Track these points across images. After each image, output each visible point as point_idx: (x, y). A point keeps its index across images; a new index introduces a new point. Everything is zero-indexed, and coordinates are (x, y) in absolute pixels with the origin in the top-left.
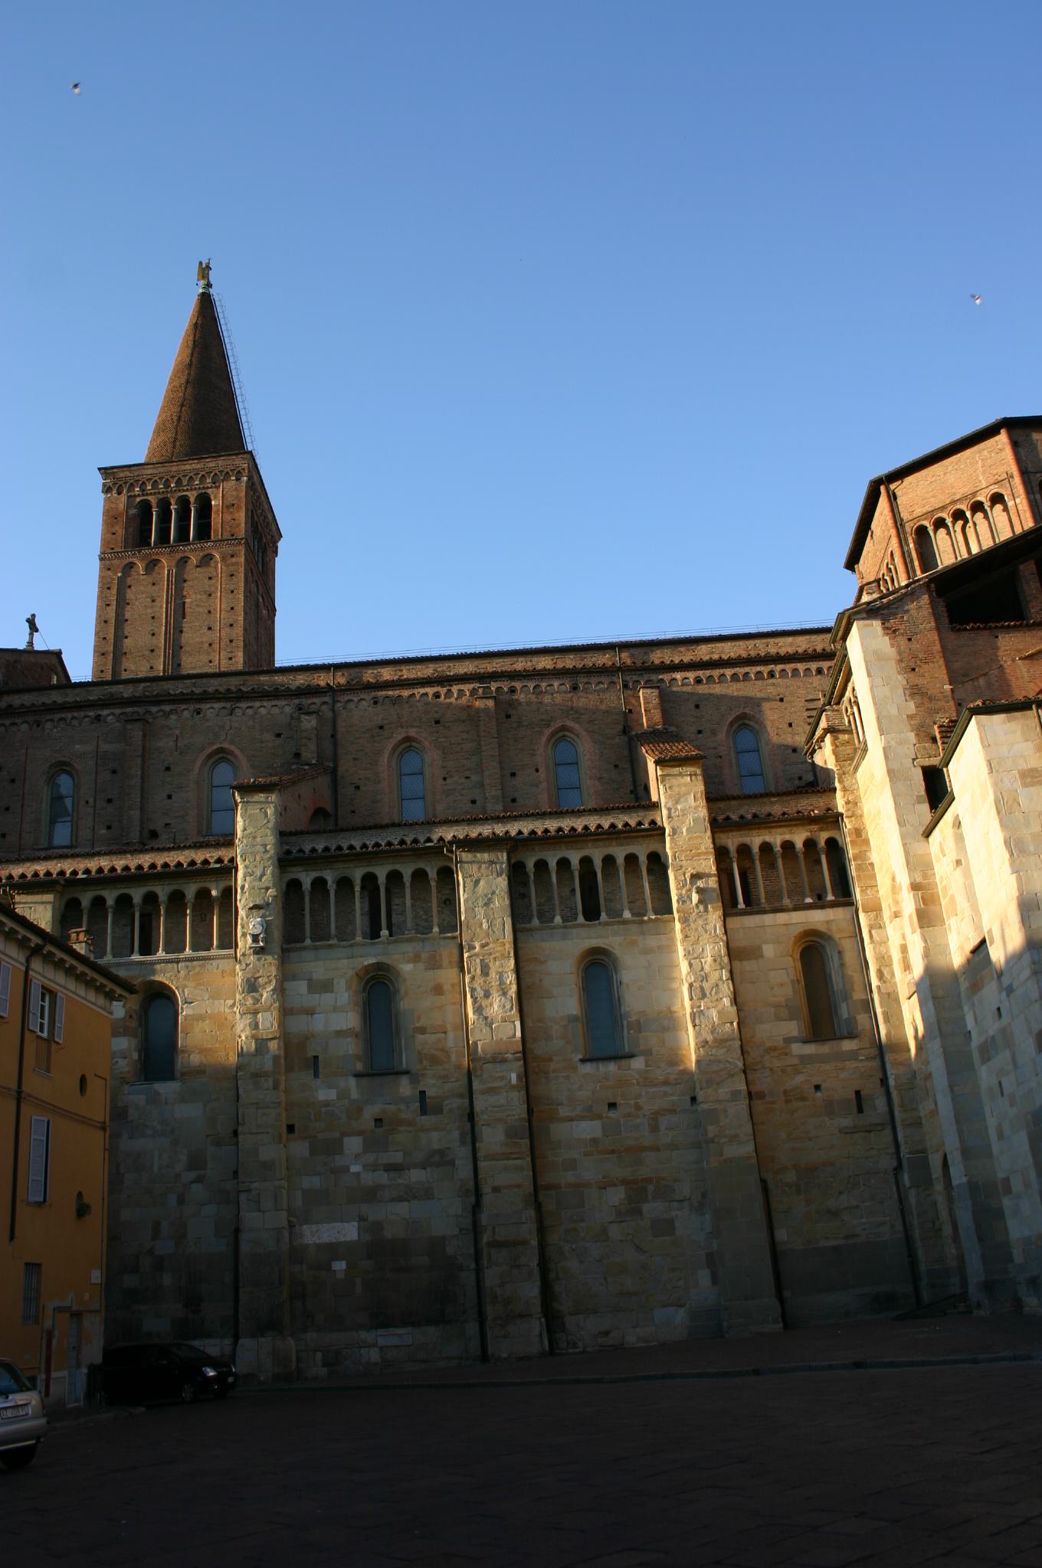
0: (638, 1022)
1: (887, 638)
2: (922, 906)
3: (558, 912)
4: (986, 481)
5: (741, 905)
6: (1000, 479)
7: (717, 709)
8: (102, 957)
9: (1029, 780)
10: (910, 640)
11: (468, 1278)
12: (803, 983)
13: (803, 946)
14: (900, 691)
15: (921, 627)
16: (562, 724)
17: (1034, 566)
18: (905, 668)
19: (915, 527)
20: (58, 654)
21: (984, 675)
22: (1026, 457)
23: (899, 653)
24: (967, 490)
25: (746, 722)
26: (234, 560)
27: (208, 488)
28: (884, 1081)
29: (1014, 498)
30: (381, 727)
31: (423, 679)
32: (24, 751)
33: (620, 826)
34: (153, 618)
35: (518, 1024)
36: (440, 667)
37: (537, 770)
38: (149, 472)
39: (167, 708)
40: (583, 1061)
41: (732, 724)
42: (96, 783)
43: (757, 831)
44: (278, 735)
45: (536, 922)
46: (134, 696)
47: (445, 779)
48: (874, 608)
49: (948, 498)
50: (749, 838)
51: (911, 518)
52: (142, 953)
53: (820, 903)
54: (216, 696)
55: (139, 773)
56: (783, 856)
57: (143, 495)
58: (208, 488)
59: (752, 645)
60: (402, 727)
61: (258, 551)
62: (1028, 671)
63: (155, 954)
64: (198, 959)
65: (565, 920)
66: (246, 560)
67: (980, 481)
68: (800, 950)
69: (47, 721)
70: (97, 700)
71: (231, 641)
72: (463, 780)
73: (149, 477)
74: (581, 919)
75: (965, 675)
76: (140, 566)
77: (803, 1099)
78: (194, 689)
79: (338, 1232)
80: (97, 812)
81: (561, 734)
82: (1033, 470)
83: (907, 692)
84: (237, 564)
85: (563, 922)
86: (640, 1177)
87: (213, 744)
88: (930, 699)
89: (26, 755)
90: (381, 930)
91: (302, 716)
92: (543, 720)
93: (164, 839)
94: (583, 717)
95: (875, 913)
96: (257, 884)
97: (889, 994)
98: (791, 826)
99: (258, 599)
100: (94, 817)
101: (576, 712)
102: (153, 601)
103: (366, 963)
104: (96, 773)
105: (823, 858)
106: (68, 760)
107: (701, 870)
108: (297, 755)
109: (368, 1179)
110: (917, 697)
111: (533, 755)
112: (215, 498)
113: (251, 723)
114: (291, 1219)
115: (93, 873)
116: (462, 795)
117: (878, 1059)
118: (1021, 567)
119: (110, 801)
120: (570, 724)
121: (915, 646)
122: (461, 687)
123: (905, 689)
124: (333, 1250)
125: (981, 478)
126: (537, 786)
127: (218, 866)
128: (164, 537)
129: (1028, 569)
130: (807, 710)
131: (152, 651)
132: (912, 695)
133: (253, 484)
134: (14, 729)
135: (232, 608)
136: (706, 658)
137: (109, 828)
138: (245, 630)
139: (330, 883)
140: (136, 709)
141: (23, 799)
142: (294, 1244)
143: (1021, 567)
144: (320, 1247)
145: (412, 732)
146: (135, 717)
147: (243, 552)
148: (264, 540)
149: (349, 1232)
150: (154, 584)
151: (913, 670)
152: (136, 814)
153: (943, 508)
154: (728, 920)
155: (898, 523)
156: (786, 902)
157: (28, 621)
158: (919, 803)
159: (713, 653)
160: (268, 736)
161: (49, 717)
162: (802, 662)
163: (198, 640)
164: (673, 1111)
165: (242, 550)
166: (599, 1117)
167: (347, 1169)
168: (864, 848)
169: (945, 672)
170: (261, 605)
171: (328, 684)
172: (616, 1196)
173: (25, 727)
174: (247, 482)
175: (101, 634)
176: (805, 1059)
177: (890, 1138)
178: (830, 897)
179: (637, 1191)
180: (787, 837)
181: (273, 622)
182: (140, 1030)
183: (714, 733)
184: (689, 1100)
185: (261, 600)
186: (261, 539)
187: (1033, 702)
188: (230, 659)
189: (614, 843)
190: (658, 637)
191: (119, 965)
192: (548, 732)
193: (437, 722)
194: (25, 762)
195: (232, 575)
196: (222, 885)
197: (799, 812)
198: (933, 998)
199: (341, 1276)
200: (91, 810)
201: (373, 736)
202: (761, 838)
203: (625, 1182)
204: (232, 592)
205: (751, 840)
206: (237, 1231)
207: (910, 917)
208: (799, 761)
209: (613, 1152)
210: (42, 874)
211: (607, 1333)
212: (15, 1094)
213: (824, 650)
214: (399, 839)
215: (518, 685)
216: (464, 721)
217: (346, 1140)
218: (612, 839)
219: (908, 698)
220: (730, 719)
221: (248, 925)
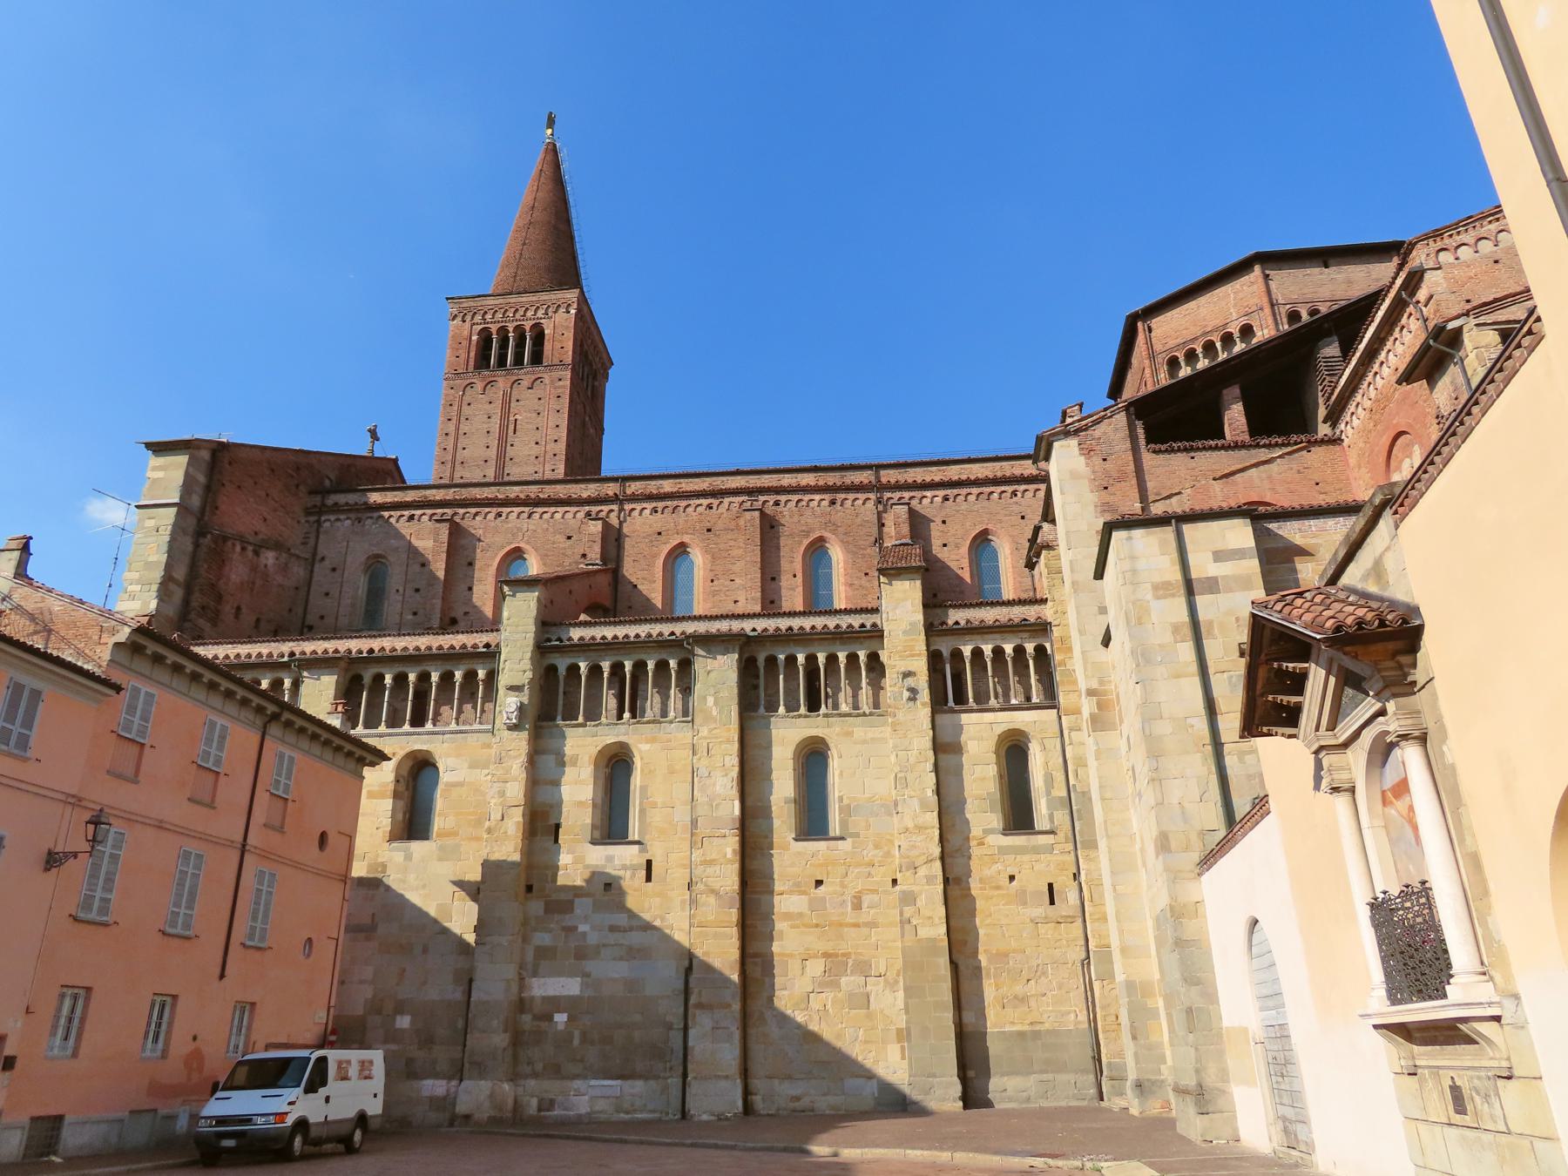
0: (849, 806)
1: (1083, 458)
2: (1096, 711)
3: (782, 703)
5: (951, 703)
6: (1250, 311)
8: (354, 728)
9: (1161, 592)
11: (676, 1039)
12: (1006, 778)
13: (1009, 744)
14: (1092, 508)
15: (1117, 448)
16: (820, 534)
18: (1098, 486)
20: (395, 461)
21: (1179, 493)
22: (1277, 289)
24: (1218, 322)
26: (561, 383)
27: (541, 319)
28: (1076, 876)
30: (659, 534)
31: (698, 491)
32: (345, 544)
33: (844, 627)
34: (488, 432)
35: (737, 804)
36: (714, 481)
37: (795, 576)
38: (492, 302)
39: (473, 510)
40: (796, 840)
41: (975, 538)
42: (406, 575)
44: (569, 538)
45: (762, 710)
46: (445, 500)
47: (712, 581)
52: (366, 726)
53: (1027, 705)
54: (516, 502)
55: (444, 566)
56: (1036, 659)
57: (485, 323)
58: (541, 319)
59: (998, 467)
60: (678, 534)
61: (588, 378)
62: (1222, 491)
63: (401, 727)
64: (461, 732)
65: (788, 710)
66: (572, 383)
67: (1231, 314)
68: (1005, 748)
69: (368, 518)
70: (412, 502)
71: (555, 455)
72: (728, 583)
73: (490, 307)
74: (803, 710)
75: (1156, 494)
76: (479, 386)
77: (998, 888)
78: (498, 494)
79: (563, 986)
80: (406, 600)
81: (819, 544)
83: (1099, 509)
84: (564, 387)
85: (787, 712)
86: (840, 952)
87: (511, 543)
89: (347, 548)
90: (624, 712)
91: (590, 521)
92: (804, 531)
93: (462, 625)
94: (839, 529)
95: (1075, 716)
96: (517, 667)
97: (1083, 793)
98: (1003, 632)
99: (584, 419)
100: (403, 604)
101: (834, 524)
102: (489, 417)
103: (609, 742)
104: (407, 565)
106: (383, 553)
107: (911, 669)
108: (584, 556)
109: (593, 939)
111: (792, 562)
112: (548, 328)
113: (545, 526)
114: (521, 971)
115: (353, 653)
116: (727, 596)
117: (1072, 853)
119: (417, 590)
120: (826, 534)
121: (1108, 465)
122: (731, 499)
123: (1096, 506)
124: (555, 1003)
126: (793, 589)
127: (484, 650)
128: (502, 362)
131: (486, 461)
133: (582, 316)
134: (339, 524)
135: (557, 426)
136: (955, 478)
137: (415, 614)
138: (568, 445)
139: (582, 669)
140: (445, 510)
141: (342, 586)
142: (523, 995)
143: (1225, 392)
144: (546, 999)
145: (686, 539)
147: (569, 376)
148: (594, 367)
149: (571, 987)
150: (490, 403)
151: (1106, 488)
152: (438, 603)
153: (1196, 339)
154: (939, 717)
155: (1152, 356)
156: (993, 702)
157: (369, 431)
160: (561, 538)
161: (369, 515)
163: (526, 453)
164: (875, 891)
165: (568, 374)
166: (804, 893)
167: (576, 928)
168: (1069, 655)
169: (1137, 490)
170: (589, 425)
171: (615, 494)
172: (816, 968)
173: (348, 522)
174: (576, 314)
175: (442, 445)
176: (1003, 850)
177: (1080, 932)
178: (1035, 700)
179: (836, 964)
181: (601, 440)
182: (406, 793)
183: (957, 547)
184: (891, 883)
185: (587, 419)
186: (591, 365)
187: (1173, 517)
188: (553, 470)
189: (838, 642)
190: (899, 459)
191: (367, 736)
192: (806, 542)
193: (709, 530)
194: (346, 553)
195: (559, 397)
196: (490, 666)
198: (1101, 799)
199: (561, 1027)
200: (401, 598)
201: (651, 541)
203: (826, 955)
204: (558, 411)
206: (471, 981)
207: (1087, 720)
209: (817, 926)
210: (331, 651)
211: (798, 1099)
212: (239, 846)
214: (646, 631)
215: (783, 498)
216: (732, 530)
217: (577, 901)
218: (837, 638)
219: (1098, 515)
221: (509, 704)
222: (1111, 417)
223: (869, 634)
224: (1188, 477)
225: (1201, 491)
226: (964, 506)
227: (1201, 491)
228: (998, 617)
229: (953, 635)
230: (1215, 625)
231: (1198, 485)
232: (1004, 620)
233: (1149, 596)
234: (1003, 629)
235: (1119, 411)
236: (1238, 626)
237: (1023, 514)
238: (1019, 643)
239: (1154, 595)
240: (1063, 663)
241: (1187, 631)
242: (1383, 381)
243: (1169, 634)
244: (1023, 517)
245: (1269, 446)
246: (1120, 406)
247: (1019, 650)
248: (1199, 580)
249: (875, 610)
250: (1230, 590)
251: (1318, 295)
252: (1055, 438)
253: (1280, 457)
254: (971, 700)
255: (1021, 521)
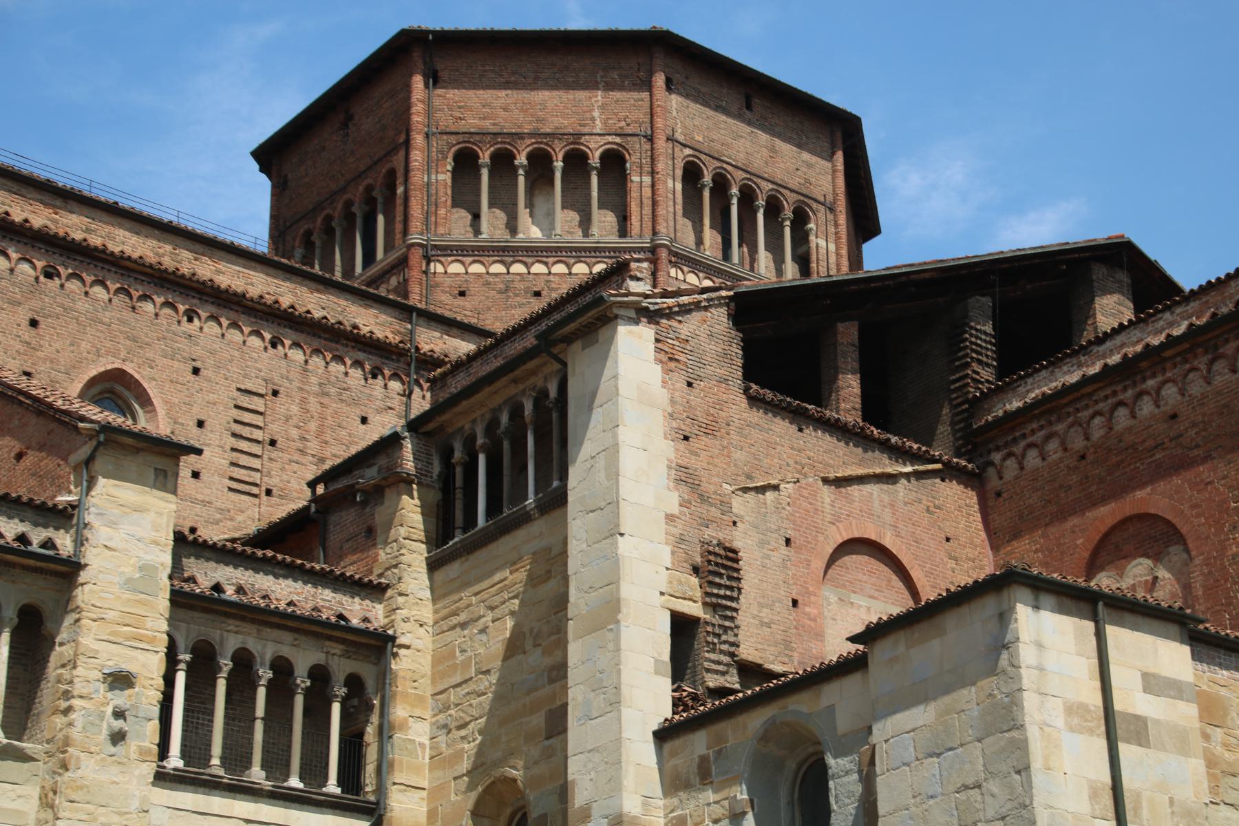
1: (659, 367)
4: (605, 122)
6: (629, 130)
7: (72, 344)
9: (1076, 721)
10: (690, 384)
17: (856, 333)
19: (470, 145)
21: (776, 488)
23: (673, 401)
25: (119, 388)
29: (641, 173)
43: (238, 623)
48: (652, 307)
49: (530, 122)
50: (218, 631)
51: (453, 129)
67: (593, 119)
75: (749, 477)
82: (681, 138)
88: (703, 498)
105: (336, 708)
110: (684, 488)
118: (841, 327)
121: (695, 397)
123: (669, 467)
125: (596, 114)
129: (848, 333)
130: (237, 407)
132: (679, 481)
143: (841, 327)
146: (541, 136)
151: (686, 438)
153: (520, 136)
158: (657, 672)
159: (88, 230)
162: (249, 315)
180: (286, 651)
197: (315, 609)
202: (240, 637)
205: (222, 636)
208: (200, 497)
213: (292, 307)
219: (672, 484)
220: (94, 373)
222: (706, 308)
223: (39, 564)
224: (791, 462)
225: (805, 493)
226: (83, 305)
227: (805, 493)
228: (295, 598)
229: (206, 610)
230: (1144, 804)
231: (803, 482)
232: (305, 609)
233: (1060, 722)
234: (306, 626)
235: (720, 302)
236: (1173, 813)
237: (198, 364)
238: (322, 663)
239: (1066, 723)
240: (404, 726)
241: (1108, 800)
242: (1131, 422)
243: (1085, 797)
244: (196, 371)
245: (885, 447)
246: (724, 293)
247: (320, 675)
248: (1126, 715)
249: (64, 516)
250: (1164, 749)
251: (731, 152)
252: (622, 312)
253: (907, 476)
254: (215, 761)
255: (192, 377)
